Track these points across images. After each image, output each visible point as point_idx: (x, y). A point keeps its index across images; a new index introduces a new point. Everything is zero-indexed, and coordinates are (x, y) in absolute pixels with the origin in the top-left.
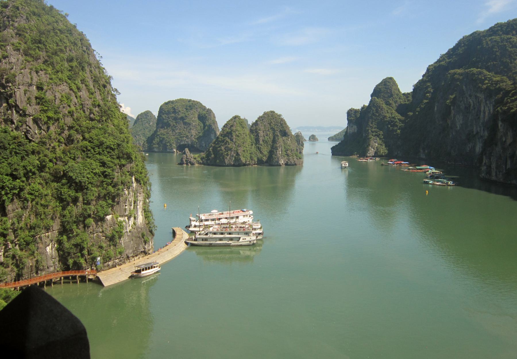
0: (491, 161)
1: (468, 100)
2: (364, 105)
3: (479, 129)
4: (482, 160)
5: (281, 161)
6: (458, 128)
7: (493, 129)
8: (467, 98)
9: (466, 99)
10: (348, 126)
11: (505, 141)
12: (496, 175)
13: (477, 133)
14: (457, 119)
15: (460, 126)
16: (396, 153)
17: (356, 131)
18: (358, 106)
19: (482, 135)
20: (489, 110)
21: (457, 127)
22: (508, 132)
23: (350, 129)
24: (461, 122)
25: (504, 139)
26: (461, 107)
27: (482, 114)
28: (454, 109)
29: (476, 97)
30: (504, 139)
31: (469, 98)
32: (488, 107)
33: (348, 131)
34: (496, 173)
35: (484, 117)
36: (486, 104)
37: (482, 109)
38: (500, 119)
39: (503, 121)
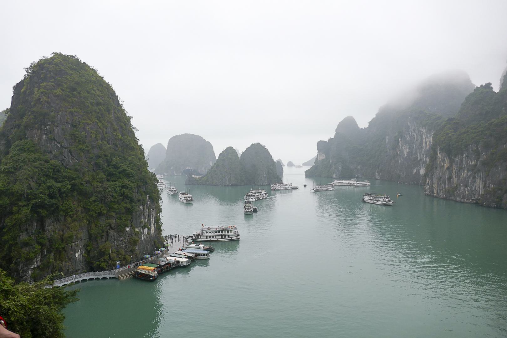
0: (433, 181)
1: (412, 133)
2: (330, 138)
3: (422, 156)
4: (426, 182)
5: (265, 182)
6: (406, 155)
7: (433, 158)
8: (411, 132)
9: (410, 133)
10: (318, 154)
11: (444, 165)
12: (437, 193)
13: (421, 159)
14: (404, 149)
15: (407, 154)
16: (357, 176)
17: (324, 158)
18: (326, 139)
19: (425, 161)
20: (430, 141)
21: (404, 155)
22: (446, 159)
23: (319, 157)
24: (408, 150)
25: (442, 164)
26: (407, 139)
27: (424, 144)
28: (401, 141)
29: (419, 131)
30: (442, 164)
31: (413, 132)
32: (429, 139)
33: (318, 158)
34: (437, 191)
35: (426, 146)
36: (427, 136)
37: (424, 140)
38: (438, 148)
39: (441, 150)
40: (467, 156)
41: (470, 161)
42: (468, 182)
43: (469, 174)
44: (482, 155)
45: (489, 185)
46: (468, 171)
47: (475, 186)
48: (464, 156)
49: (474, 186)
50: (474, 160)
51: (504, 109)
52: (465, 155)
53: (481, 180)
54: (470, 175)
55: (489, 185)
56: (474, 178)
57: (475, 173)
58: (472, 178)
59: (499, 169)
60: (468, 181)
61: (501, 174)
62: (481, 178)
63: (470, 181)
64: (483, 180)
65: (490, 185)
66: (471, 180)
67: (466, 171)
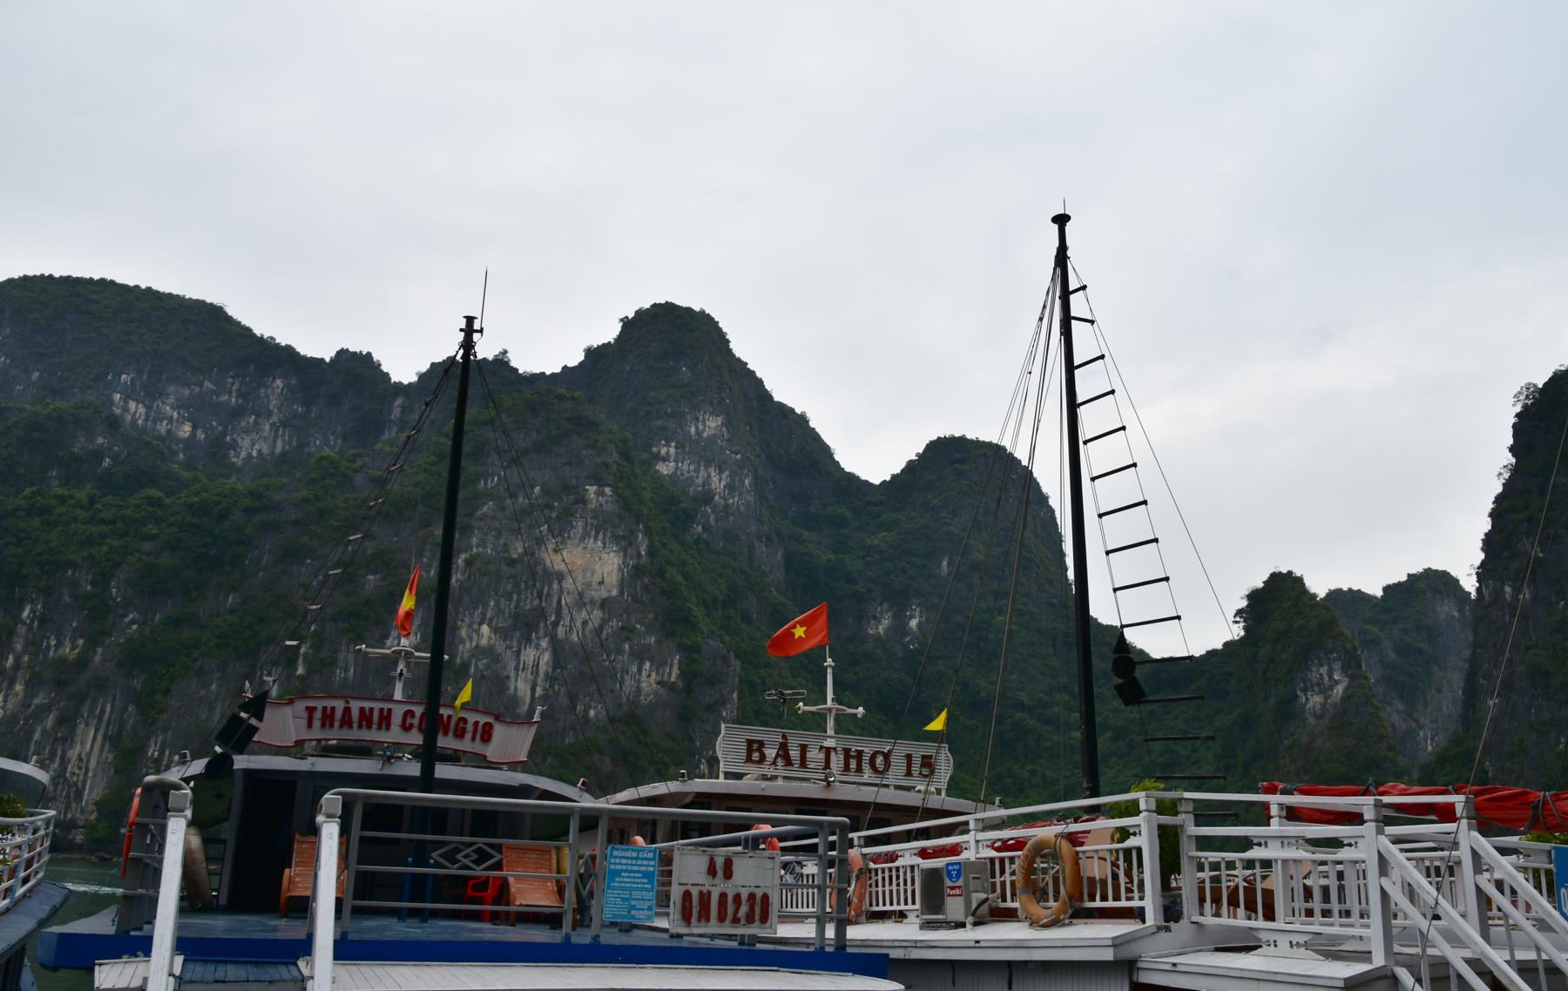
40: (43, 620)
41: (53, 643)
42: (30, 739)
43: (37, 701)
44: (126, 620)
45: (162, 752)
46: (33, 685)
47: (63, 758)
48: (25, 614)
49: (58, 759)
50: (73, 640)
51: (54, 473)
52: (33, 611)
53: (101, 731)
54: (44, 710)
55: (162, 752)
56: (68, 721)
57: (82, 698)
58: (50, 721)
59: (213, 687)
60: (31, 732)
61: (218, 711)
62: (104, 724)
63: (37, 736)
64: (110, 733)
65: (167, 753)
66: (44, 731)
67: (19, 687)
